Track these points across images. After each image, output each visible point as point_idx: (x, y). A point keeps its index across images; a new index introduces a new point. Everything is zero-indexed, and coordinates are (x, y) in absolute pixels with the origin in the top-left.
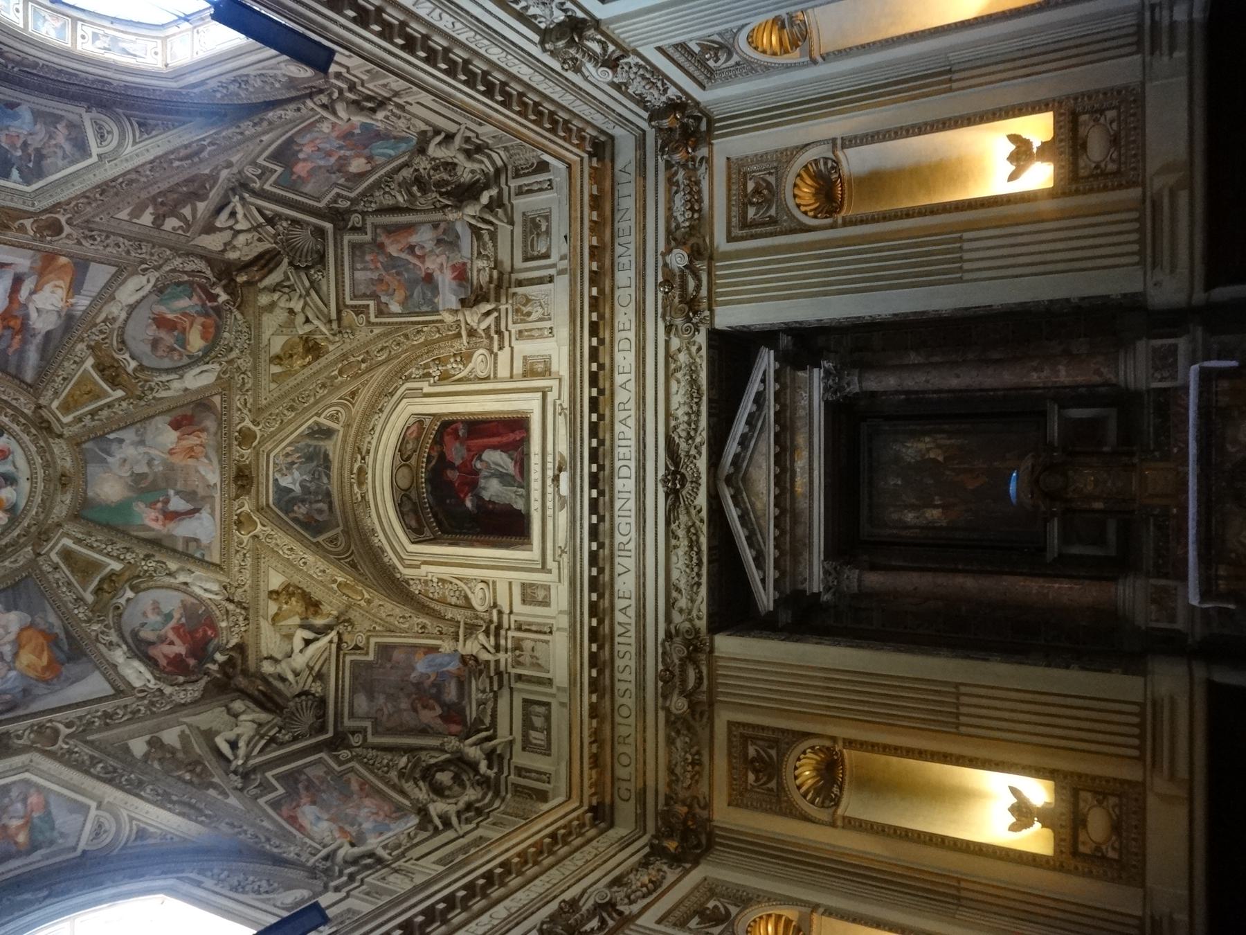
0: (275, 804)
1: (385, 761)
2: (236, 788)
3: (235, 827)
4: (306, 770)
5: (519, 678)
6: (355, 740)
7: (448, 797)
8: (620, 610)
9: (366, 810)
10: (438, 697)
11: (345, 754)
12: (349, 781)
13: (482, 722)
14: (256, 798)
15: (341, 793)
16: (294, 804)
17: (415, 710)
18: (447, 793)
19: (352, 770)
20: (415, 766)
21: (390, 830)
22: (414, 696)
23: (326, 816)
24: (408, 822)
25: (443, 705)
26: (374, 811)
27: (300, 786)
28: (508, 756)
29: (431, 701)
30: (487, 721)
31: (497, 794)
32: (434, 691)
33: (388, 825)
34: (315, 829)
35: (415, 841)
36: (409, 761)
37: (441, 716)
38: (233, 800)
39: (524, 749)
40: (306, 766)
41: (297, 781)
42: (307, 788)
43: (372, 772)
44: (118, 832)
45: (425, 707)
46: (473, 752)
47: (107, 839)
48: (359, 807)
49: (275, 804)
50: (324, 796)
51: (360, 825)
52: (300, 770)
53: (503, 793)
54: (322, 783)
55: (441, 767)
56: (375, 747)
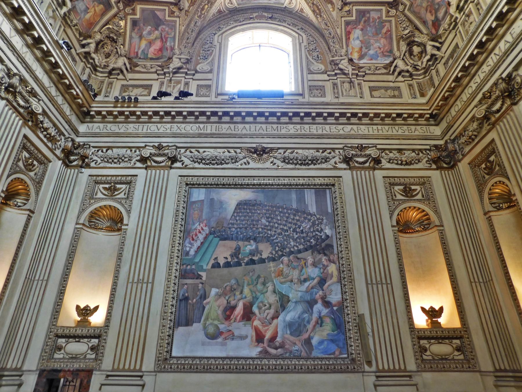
0: (347, 23)
1: (404, 26)
2: (338, 8)
3: (327, 25)
4: (371, 12)
5: (460, 32)
6: (401, 8)
7: (412, 59)
8: (506, 41)
9: (378, 44)
10: (437, 11)
11: (393, 12)
12: (384, 26)
13: (441, 38)
14: (342, 17)
15: (376, 31)
16: (355, 26)
17: (427, 10)
18: (412, 57)
19: (390, 21)
20: (410, 37)
21: (376, 59)
22: (429, 3)
23: (361, 39)
24: (385, 60)
25: (436, 17)
26: (381, 46)
27: (363, 19)
28: (438, 62)
29: (433, 11)
30: (443, 39)
31: (425, 73)
32: (437, 7)
33: (378, 57)
34: (353, 42)
35: (377, 72)
36: (409, 33)
37: (433, 21)
38: (334, 14)
39: (444, 64)
40: (373, 10)
41: (364, 16)
42: (365, 22)
43: (396, 27)
44: (296, 5)
45: (430, 12)
46: (429, 48)
47: (292, 6)
48: (377, 41)
49: (347, 23)
50: (369, 28)
51: (370, 50)
52: (369, 11)
53: (427, 74)
54: (373, 22)
55: (419, 45)
56: (405, 16)
